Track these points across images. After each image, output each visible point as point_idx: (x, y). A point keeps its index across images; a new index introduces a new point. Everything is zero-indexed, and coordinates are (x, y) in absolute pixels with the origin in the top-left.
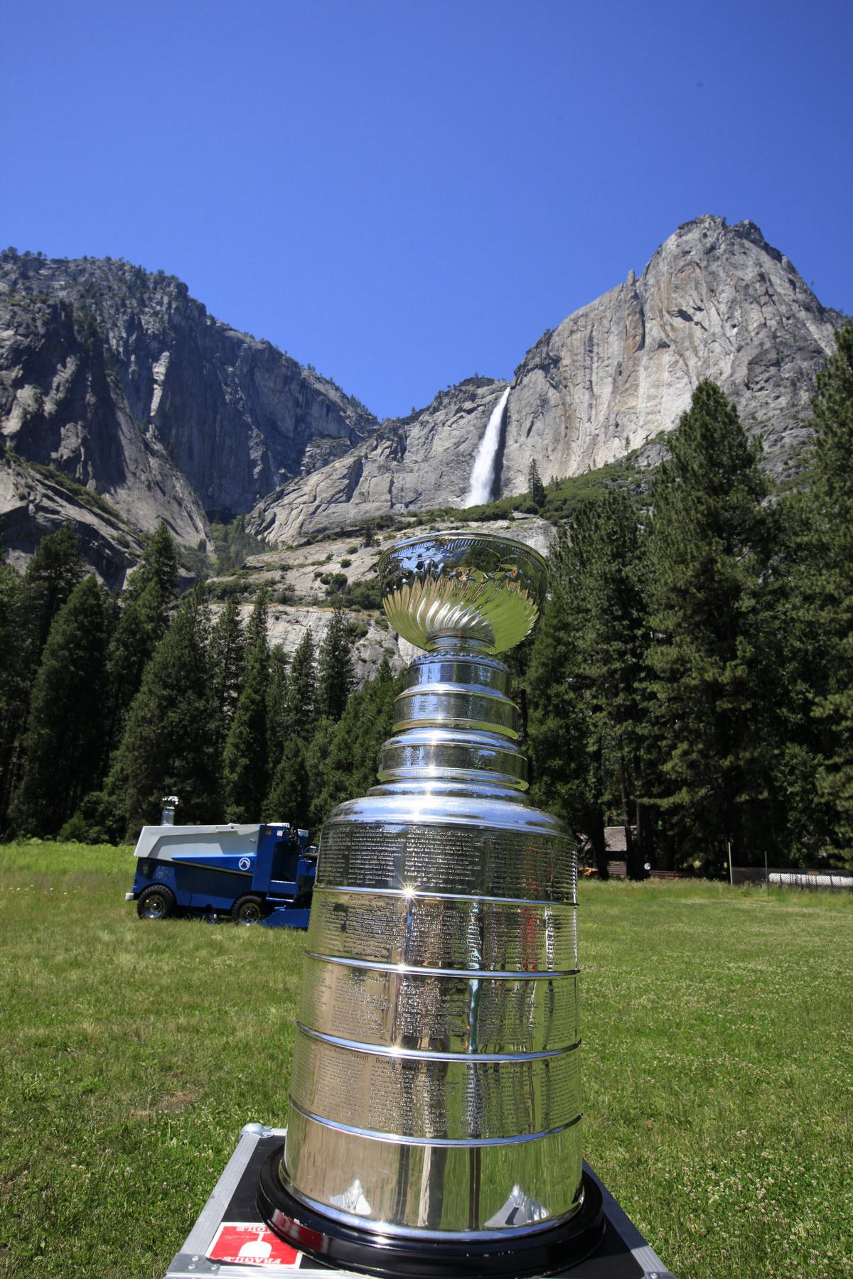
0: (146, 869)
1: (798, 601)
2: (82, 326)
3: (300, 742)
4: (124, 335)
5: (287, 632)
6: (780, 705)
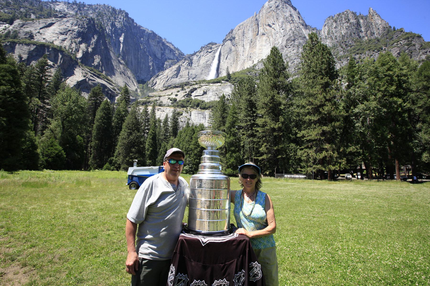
0: (130, 178)
1: (295, 107)
3: (166, 143)
4: (111, 28)
5: (161, 114)
6: (289, 134)
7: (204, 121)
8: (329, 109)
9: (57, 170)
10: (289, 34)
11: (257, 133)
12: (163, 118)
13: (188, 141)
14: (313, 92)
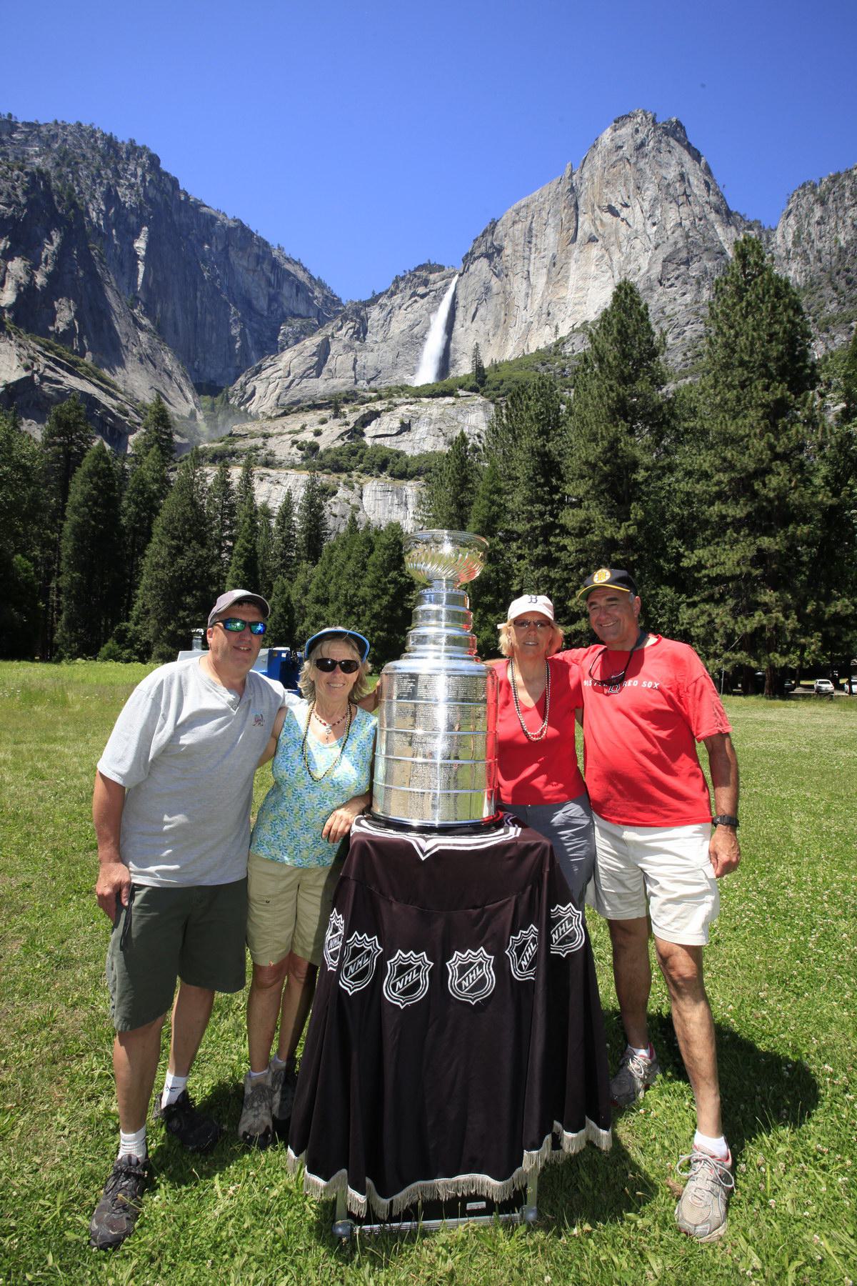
1: (679, 475)
3: (286, 582)
5: (270, 491)
6: (658, 557)
7: (401, 514)
8: (782, 485)
10: (671, 241)
11: (563, 555)
12: (276, 504)
13: (355, 575)
14: (737, 429)
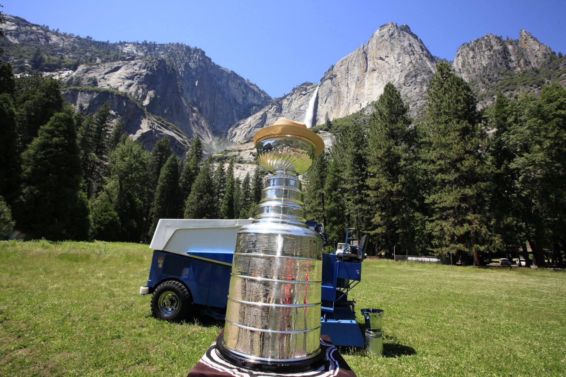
2: (169, 68)
3: (245, 211)
5: (240, 173)
6: (413, 199)
9: (109, 242)
10: (408, 68)
11: (368, 199)
14: (446, 140)
